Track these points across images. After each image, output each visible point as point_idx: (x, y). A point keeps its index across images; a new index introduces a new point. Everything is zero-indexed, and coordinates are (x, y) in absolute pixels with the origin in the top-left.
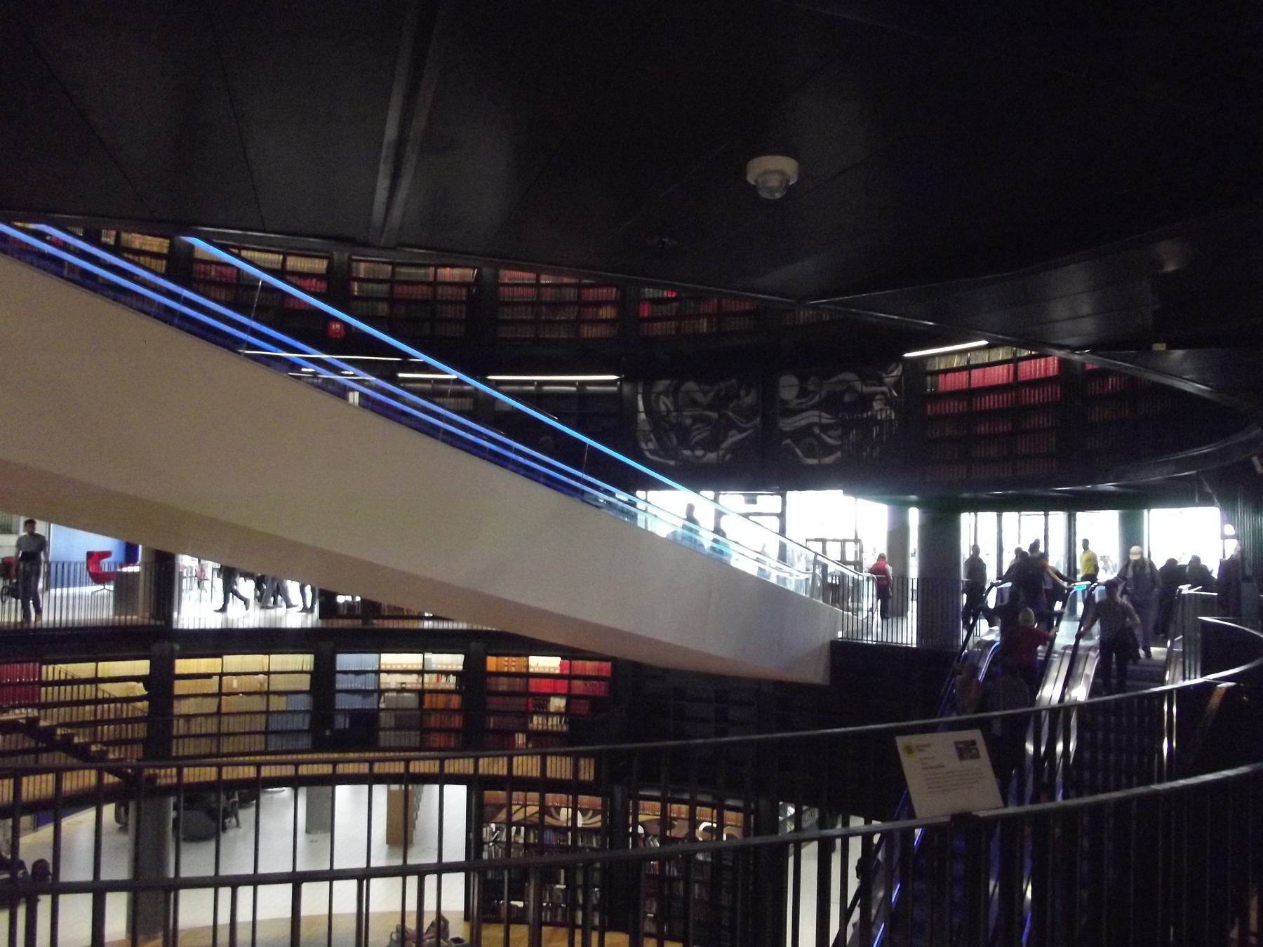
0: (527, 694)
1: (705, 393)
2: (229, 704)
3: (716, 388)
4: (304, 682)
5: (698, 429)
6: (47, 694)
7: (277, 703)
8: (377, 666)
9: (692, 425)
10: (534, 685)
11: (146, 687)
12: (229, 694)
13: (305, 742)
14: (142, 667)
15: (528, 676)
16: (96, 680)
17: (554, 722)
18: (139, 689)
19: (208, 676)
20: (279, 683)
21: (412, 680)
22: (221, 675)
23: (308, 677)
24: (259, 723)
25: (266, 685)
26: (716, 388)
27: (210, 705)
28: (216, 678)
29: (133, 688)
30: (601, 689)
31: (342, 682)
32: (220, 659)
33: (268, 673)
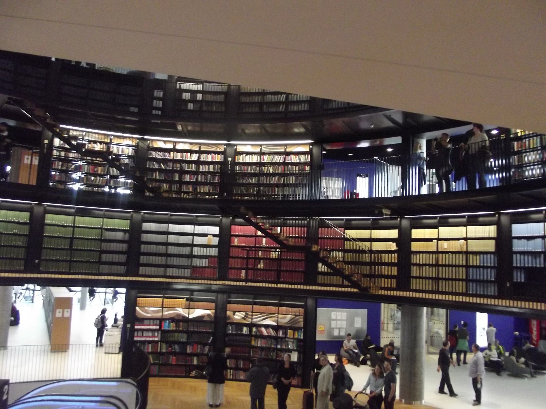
2: (443, 259)
4: (491, 246)
6: (348, 245)
7: (474, 261)
8: (543, 232)
11: (397, 246)
12: (443, 252)
13: (492, 290)
14: (394, 233)
16: (371, 240)
18: (393, 246)
19: (430, 240)
20: (474, 246)
22: (438, 239)
23: (493, 242)
24: (462, 273)
25: (465, 247)
27: (432, 259)
28: (435, 241)
29: (390, 245)
31: (518, 246)
32: (437, 230)
33: (466, 239)
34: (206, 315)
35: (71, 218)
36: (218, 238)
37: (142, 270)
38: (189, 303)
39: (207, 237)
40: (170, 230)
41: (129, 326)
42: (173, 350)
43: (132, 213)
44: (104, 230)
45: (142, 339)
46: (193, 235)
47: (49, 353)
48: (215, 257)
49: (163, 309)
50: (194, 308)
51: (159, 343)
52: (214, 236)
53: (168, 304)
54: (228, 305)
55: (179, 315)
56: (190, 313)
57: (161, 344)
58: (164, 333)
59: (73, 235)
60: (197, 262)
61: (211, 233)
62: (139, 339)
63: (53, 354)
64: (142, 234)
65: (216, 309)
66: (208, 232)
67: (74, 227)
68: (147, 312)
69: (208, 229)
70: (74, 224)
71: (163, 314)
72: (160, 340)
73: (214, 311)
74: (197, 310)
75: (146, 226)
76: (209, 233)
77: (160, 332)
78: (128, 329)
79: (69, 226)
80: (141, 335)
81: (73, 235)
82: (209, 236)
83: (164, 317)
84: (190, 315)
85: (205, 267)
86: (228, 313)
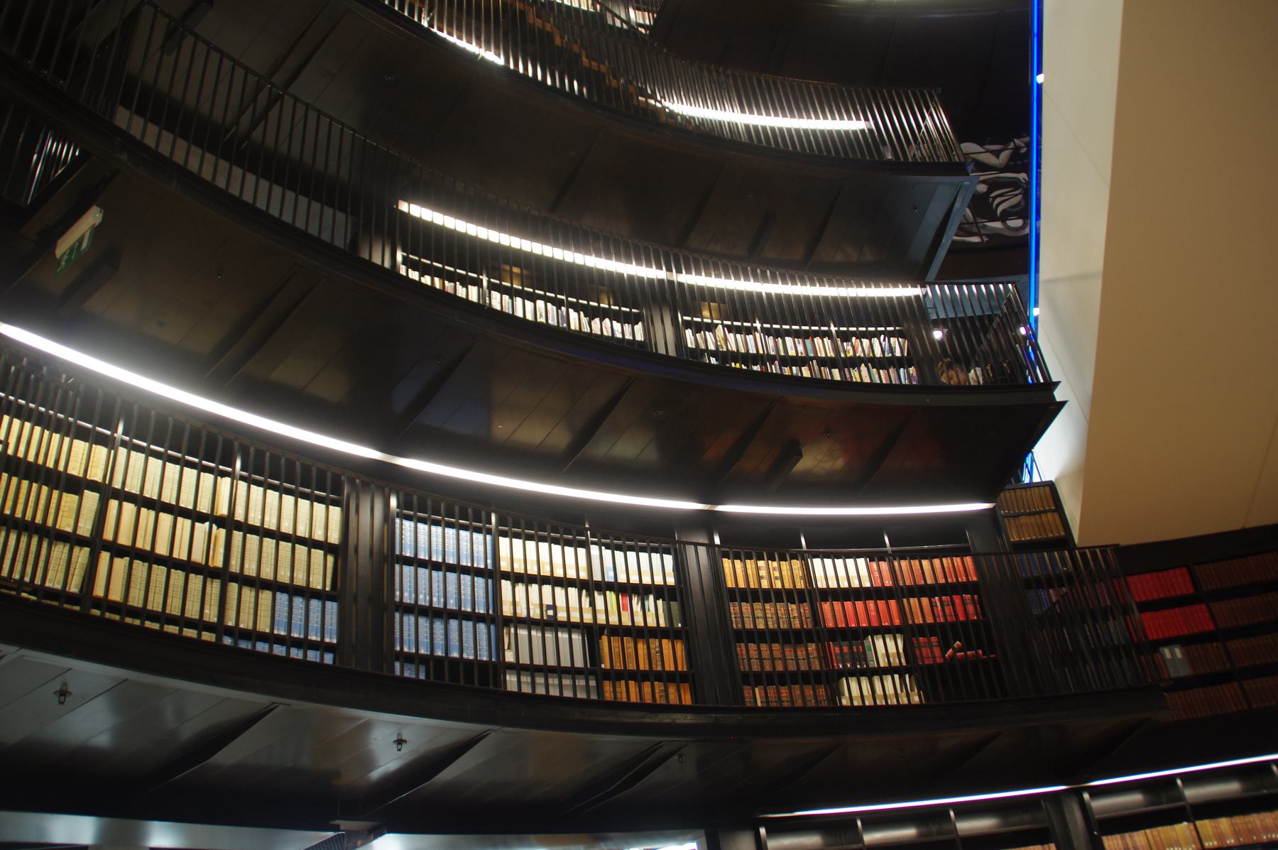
0: (818, 634)
1: (997, 154)
3: (1012, 145)
5: (1001, 195)
9: (990, 191)
10: (831, 613)
15: (812, 596)
17: (889, 690)
21: (570, 604)
26: (1012, 145)
30: (966, 608)
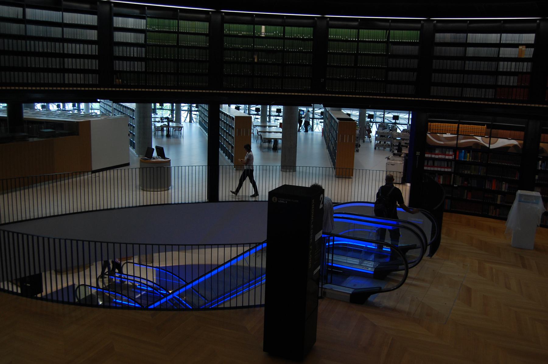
34: (511, 146)
35: (354, 31)
36: (533, 49)
37: (434, 90)
38: (491, 131)
39: (518, 47)
40: (469, 41)
41: (418, 153)
42: (469, 185)
43: (422, 22)
44: (390, 44)
45: (432, 169)
46: (499, 45)
47: (334, 178)
48: (527, 73)
49: (458, 137)
50: (498, 137)
51: (453, 175)
52: (528, 46)
53: (465, 130)
54: (542, 135)
55: (477, 144)
56: (491, 143)
57: (454, 176)
58: (458, 164)
59: (357, 51)
60: (502, 80)
61: (523, 42)
62: (429, 168)
63: (337, 179)
64: (435, 48)
65: (525, 140)
66: (519, 41)
67: (358, 41)
68: (439, 139)
69: (519, 37)
70: (358, 38)
71: (458, 142)
72: (453, 171)
73: (522, 142)
74: (499, 140)
75: (440, 37)
76: (520, 42)
77: (453, 163)
78: (418, 157)
79: (353, 41)
80: (432, 164)
81: (357, 51)
82: (520, 47)
83: (458, 146)
84: (491, 145)
85: (513, 87)
86: (541, 145)
